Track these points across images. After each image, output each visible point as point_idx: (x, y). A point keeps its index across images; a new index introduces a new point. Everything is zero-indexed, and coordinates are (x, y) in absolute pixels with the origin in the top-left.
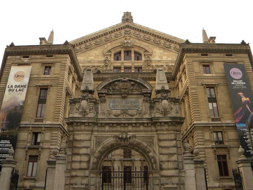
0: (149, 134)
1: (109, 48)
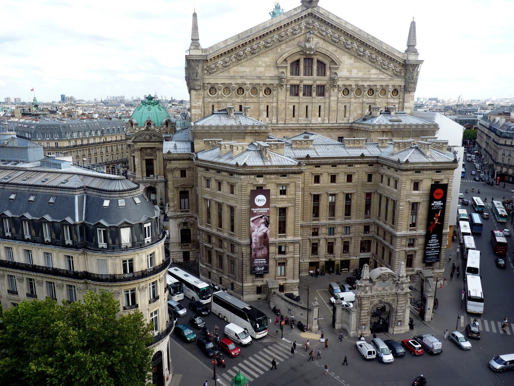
0: (393, 298)
1: (285, 56)
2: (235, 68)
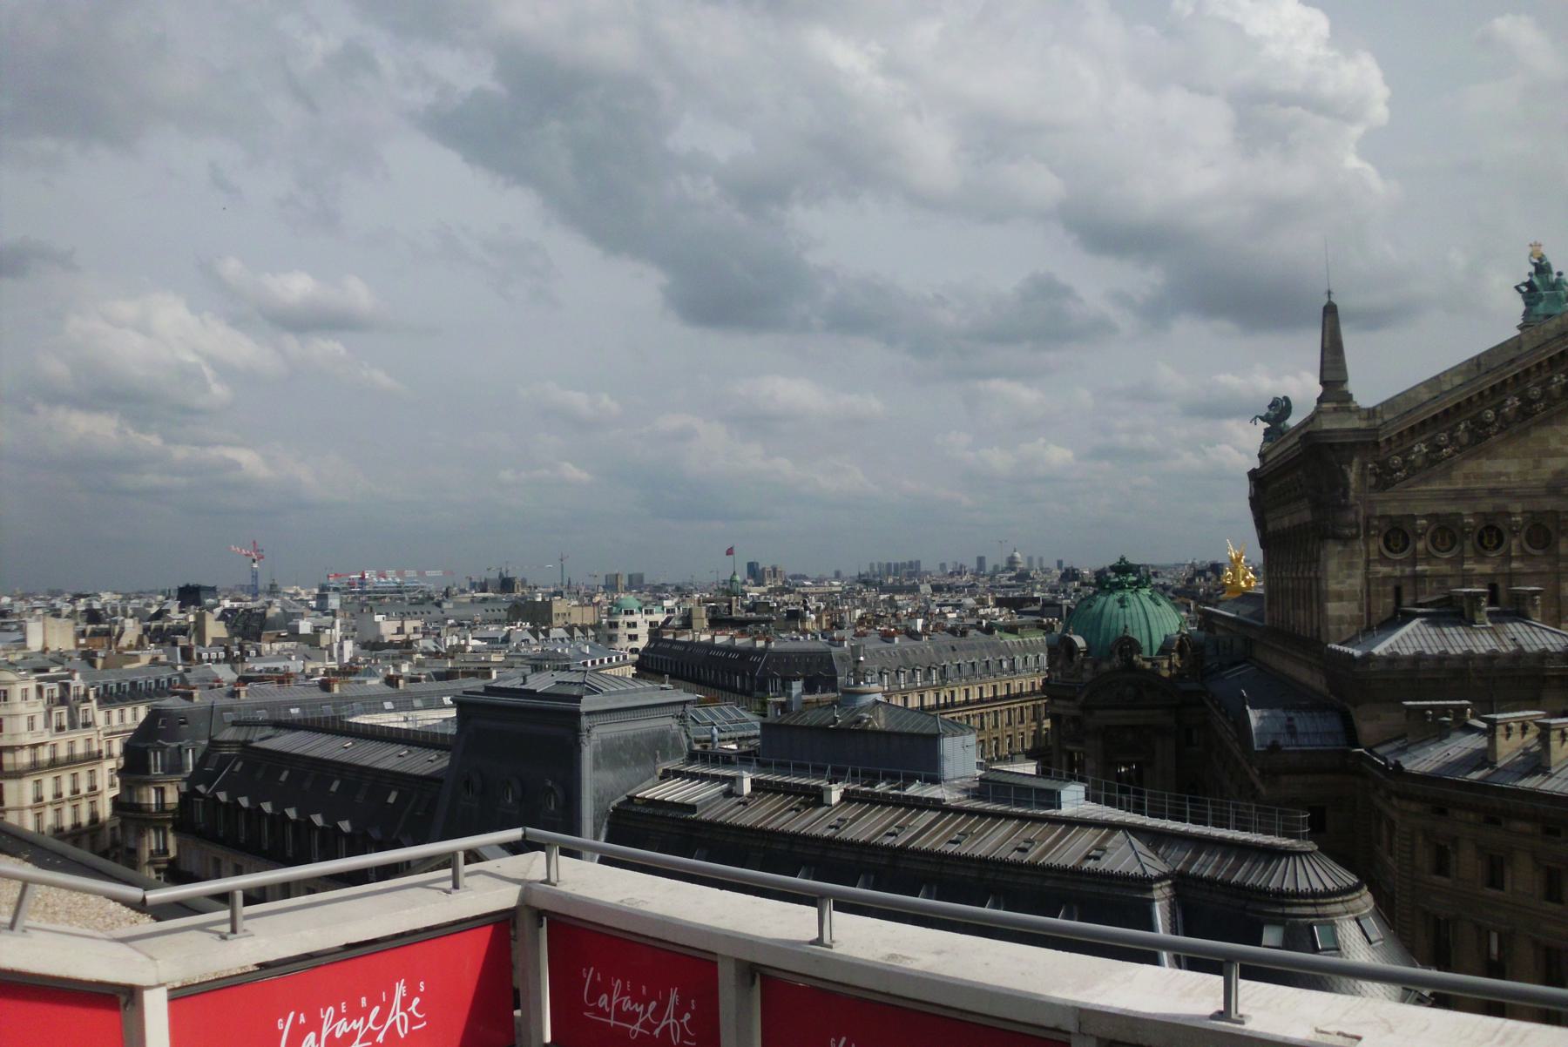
2: (1471, 466)
